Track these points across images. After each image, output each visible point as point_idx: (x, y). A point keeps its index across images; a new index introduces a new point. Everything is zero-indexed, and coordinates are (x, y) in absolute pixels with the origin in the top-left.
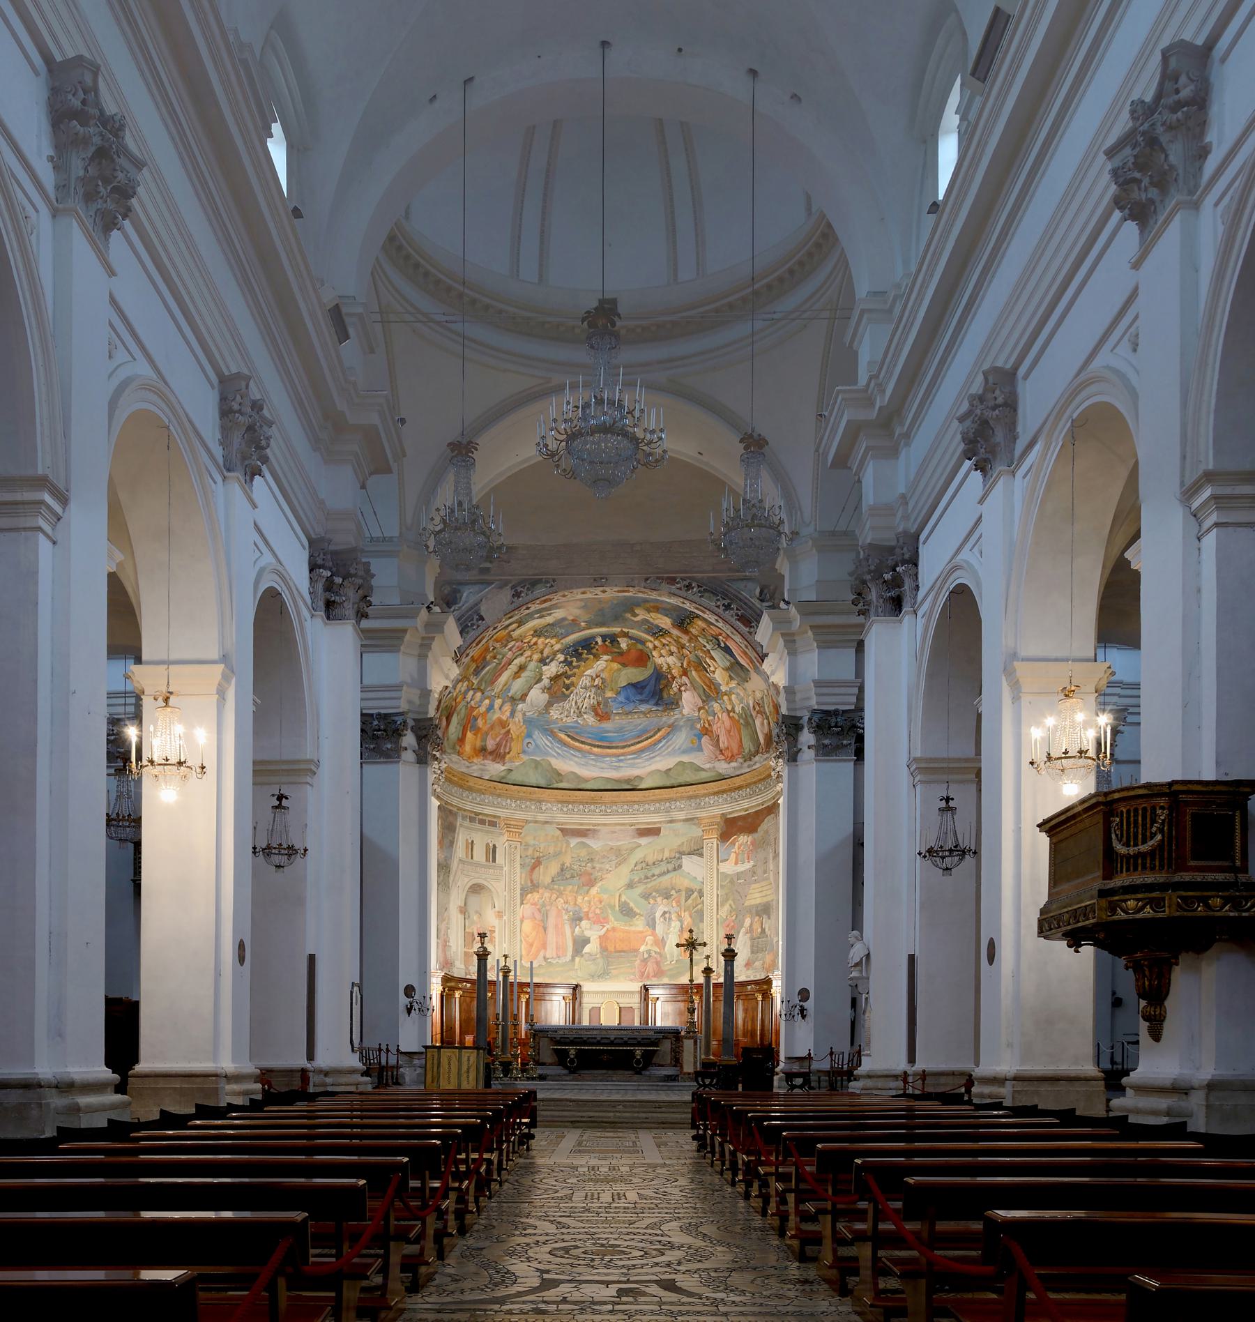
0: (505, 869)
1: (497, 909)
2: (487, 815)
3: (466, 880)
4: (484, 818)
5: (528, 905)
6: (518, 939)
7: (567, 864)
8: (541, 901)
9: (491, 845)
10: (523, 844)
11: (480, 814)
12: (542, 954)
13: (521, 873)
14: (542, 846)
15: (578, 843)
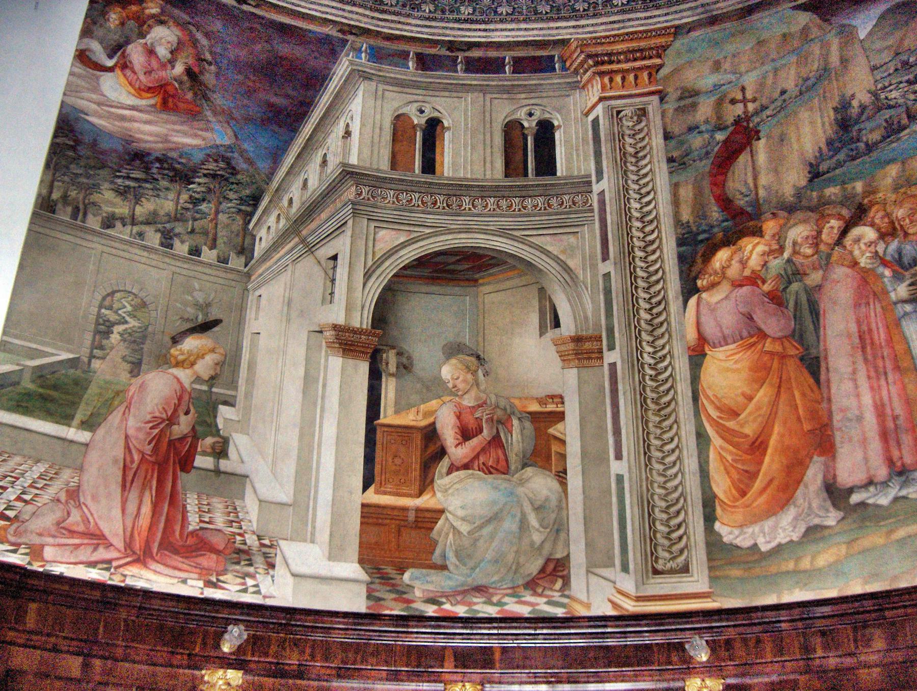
0: (596, 188)
1: (568, 327)
2: (499, 45)
3: (387, 238)
4: (493, 54)
5: (724, 290)
6: (687, 431)
7: (863, 97)
8: (776, 264)
9: (530, 124)
10: (673, 95)
11: (471, 46)
12: (814, 474)
13: (675, 187)
14: (750, 80)
15: (883, 17)
